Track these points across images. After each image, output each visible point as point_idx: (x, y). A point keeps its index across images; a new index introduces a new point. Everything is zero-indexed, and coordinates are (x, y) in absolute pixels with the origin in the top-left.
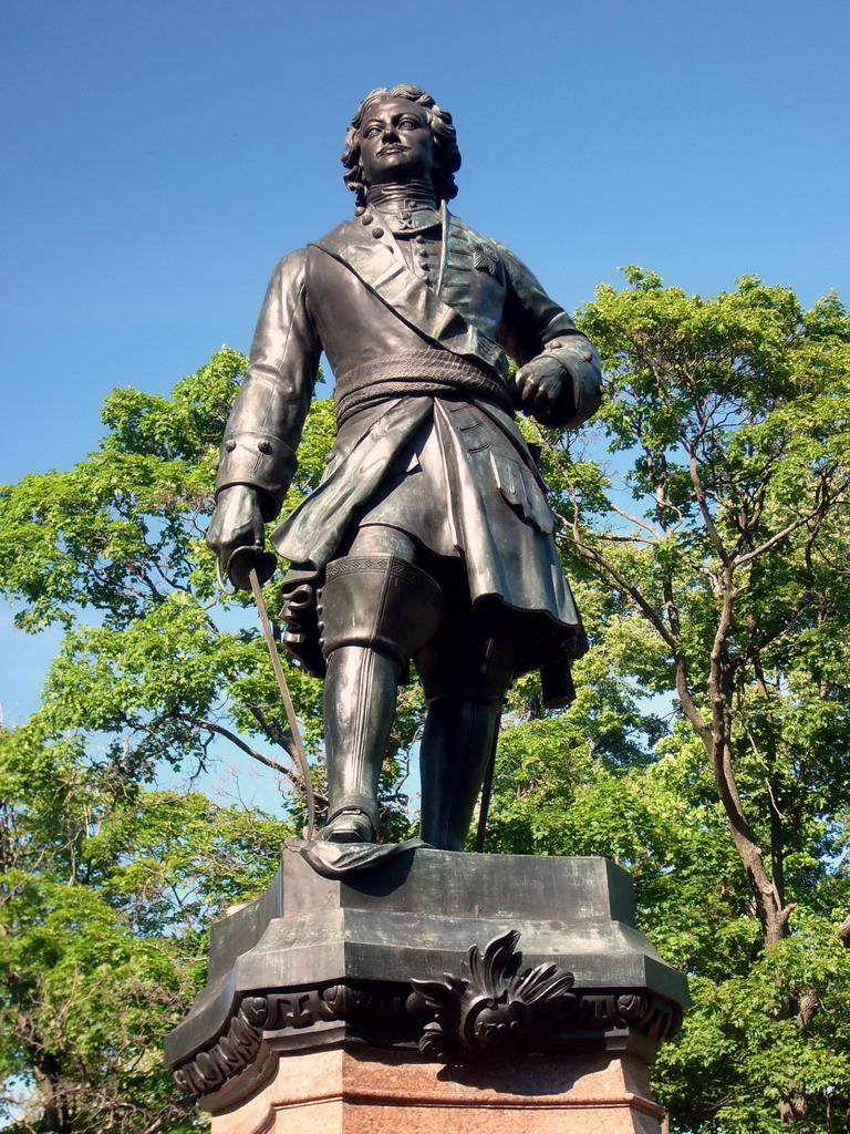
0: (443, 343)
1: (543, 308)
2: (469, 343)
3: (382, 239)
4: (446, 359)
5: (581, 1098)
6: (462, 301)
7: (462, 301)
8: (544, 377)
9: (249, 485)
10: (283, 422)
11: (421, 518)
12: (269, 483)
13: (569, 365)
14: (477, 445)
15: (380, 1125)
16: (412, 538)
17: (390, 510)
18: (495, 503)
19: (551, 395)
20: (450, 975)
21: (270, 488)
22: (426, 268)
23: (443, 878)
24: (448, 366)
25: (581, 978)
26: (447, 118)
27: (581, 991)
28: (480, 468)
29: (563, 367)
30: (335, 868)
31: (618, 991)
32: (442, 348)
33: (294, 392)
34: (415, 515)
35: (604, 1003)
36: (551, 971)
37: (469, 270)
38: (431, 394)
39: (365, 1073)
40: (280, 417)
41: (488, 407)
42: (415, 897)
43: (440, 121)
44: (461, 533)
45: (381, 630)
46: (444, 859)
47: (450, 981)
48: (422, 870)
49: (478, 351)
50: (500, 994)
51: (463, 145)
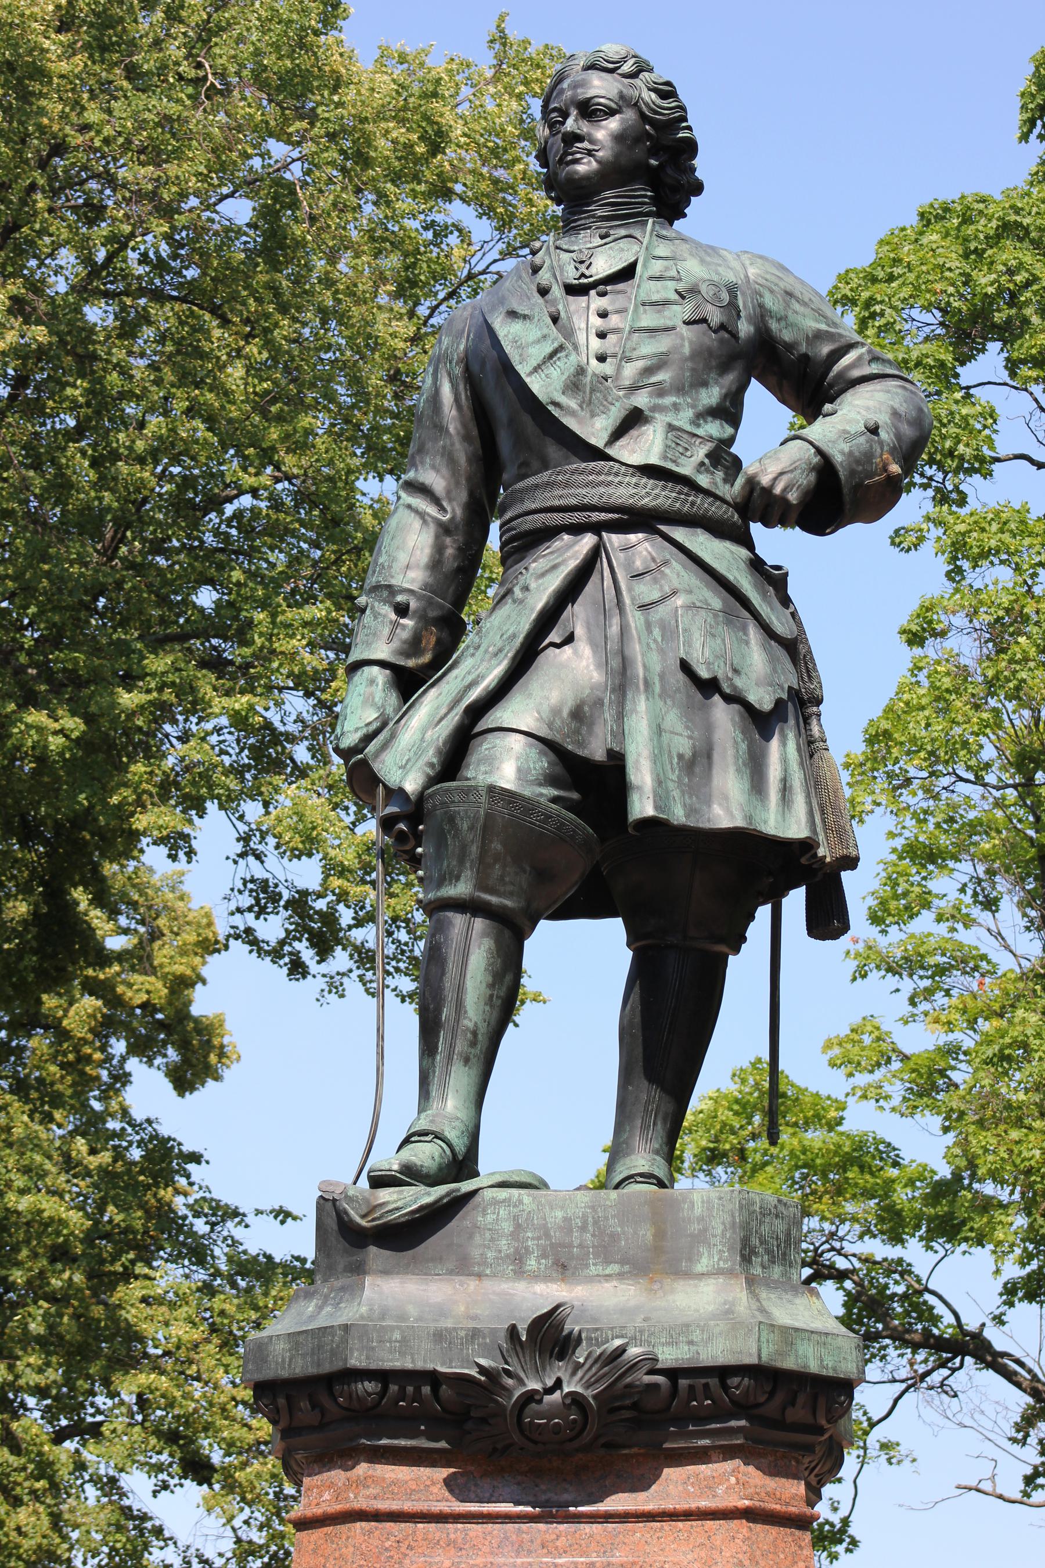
0: (609, 451)
1: (825, 349)
2: (646, 446)
3: (549, 297)
4: (617, 474)
5: (669, 1506)
6: (654, 379)
7: (654, 379)
8: (781, 474)
9: (382, 664)
10: (435, 564)
11: (565, 713)
12: (408, 655)
13: (824, 447)
14: (656, 595)
15: (410, 1547)
16: (548, 744)
17: (521, 711)
18: (681, 676)
19: (793, 497)
20: (483, 1362)
21: (411, 663)
22: (602, 335)
23: (518, 1227)
24: (620, 483)
25: (669, 1356)
26: (667, 92)
27: (673, 1374)
28: (657, 632)
29: (819, 451)
30: (364, 1223)
31: (724, 1372)
32: (608, 458)
33: (453, 519)
34: (556, 712)
35: (706, 1386)
36: (621, 1351)
37: (673, 328)
38: (597, 528)
39: (394, 1483)
40: (432, 556)
41: (679, 534)
42: (476, 1253)
43: (653, 95)
44: (620, 734)
45: (482, 885)
46: (521, 1202)
47: (482, 1370)
48: (490, 1218)
49: (665, 458)
50: (550, 1383)
51: (701, 125)
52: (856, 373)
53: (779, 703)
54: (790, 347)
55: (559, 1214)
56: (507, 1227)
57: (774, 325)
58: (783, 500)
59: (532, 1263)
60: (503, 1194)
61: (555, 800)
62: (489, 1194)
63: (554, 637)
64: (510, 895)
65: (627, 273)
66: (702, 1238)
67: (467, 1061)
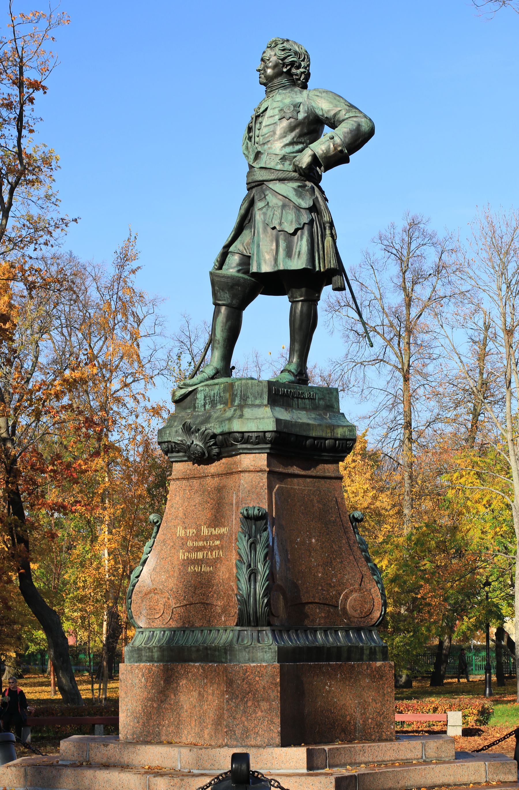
23: (205, 397)
41: (271, 185)
42: (197, 405)
52: (341, 119)
53: (296, 230)
54: (323, 116)
55: (213, 392)
56: (203, 397)
57: (317, 111)
58: (301, 167)
59: (207, 407)
60: (202, 388)
61: (239, 271)
62: (199, 389)
63: (247, 222)
64: (225, 300)
65: (266, 109)
66: (236, 395)
67: (217, 349)
